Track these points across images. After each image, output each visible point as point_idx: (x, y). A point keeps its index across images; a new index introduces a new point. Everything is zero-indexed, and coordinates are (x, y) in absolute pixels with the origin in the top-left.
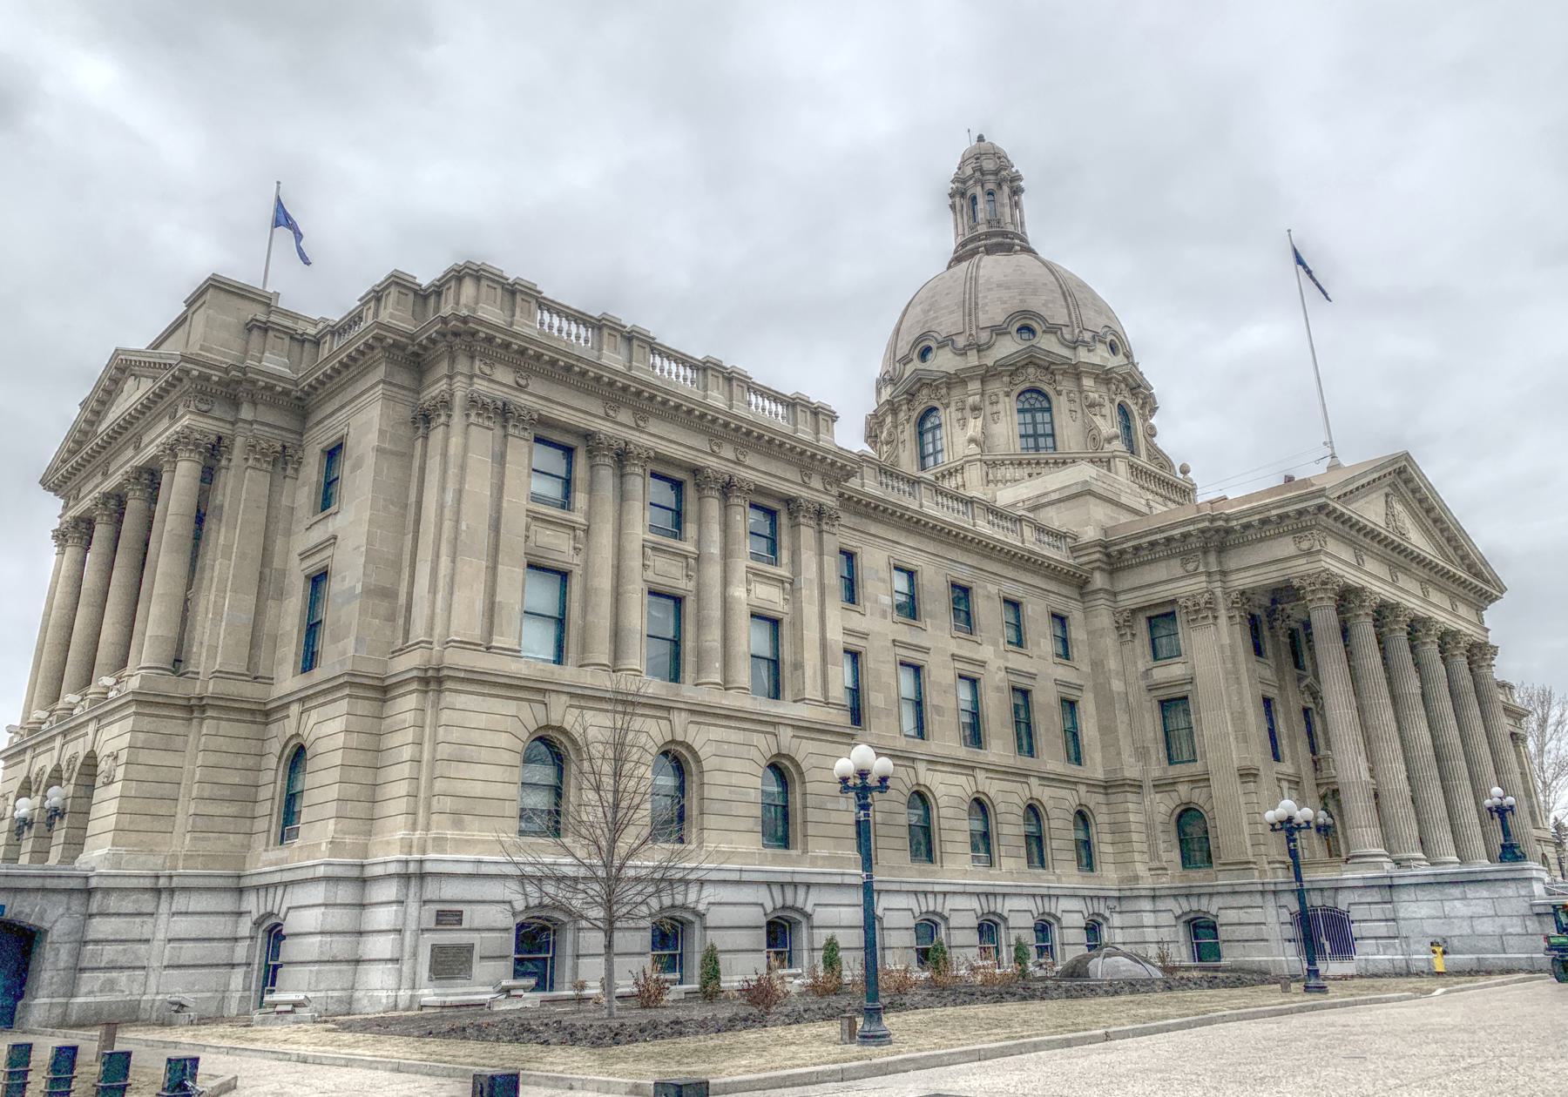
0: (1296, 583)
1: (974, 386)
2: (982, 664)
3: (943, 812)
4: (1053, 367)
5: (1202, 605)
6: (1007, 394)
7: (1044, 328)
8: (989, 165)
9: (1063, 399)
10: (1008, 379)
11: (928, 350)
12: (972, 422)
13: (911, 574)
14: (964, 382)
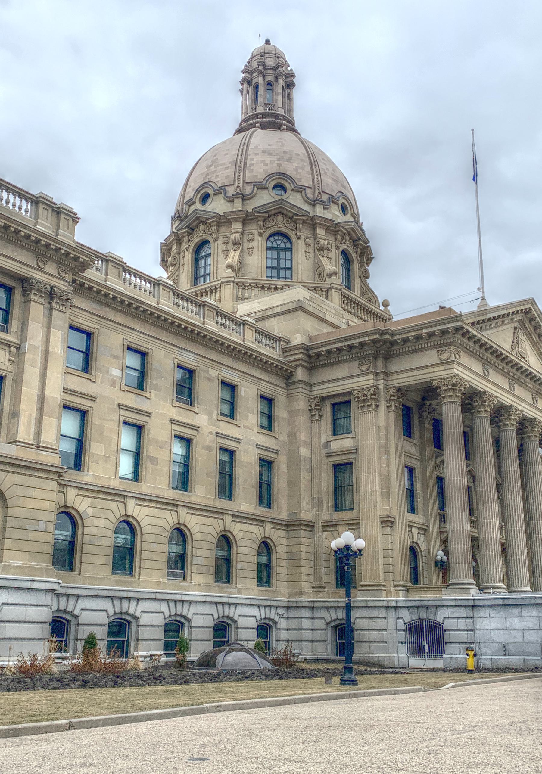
0: (435, 384)
1: (237, 226)
2: (196, 428)
3: (146, 538)
5: (369, 397)
6: (260, 235)
7: (293, 188)
8: (270, 62)
9: (301, 242)
10: (262, 223)
12: (232, 253)
13: (143, 355)
14: (229, 222)
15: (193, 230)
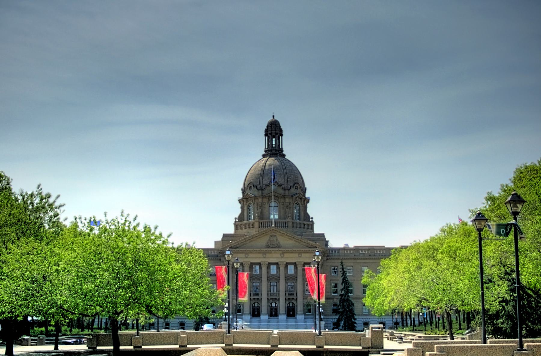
1: (260, 200)
11: (251, 187)
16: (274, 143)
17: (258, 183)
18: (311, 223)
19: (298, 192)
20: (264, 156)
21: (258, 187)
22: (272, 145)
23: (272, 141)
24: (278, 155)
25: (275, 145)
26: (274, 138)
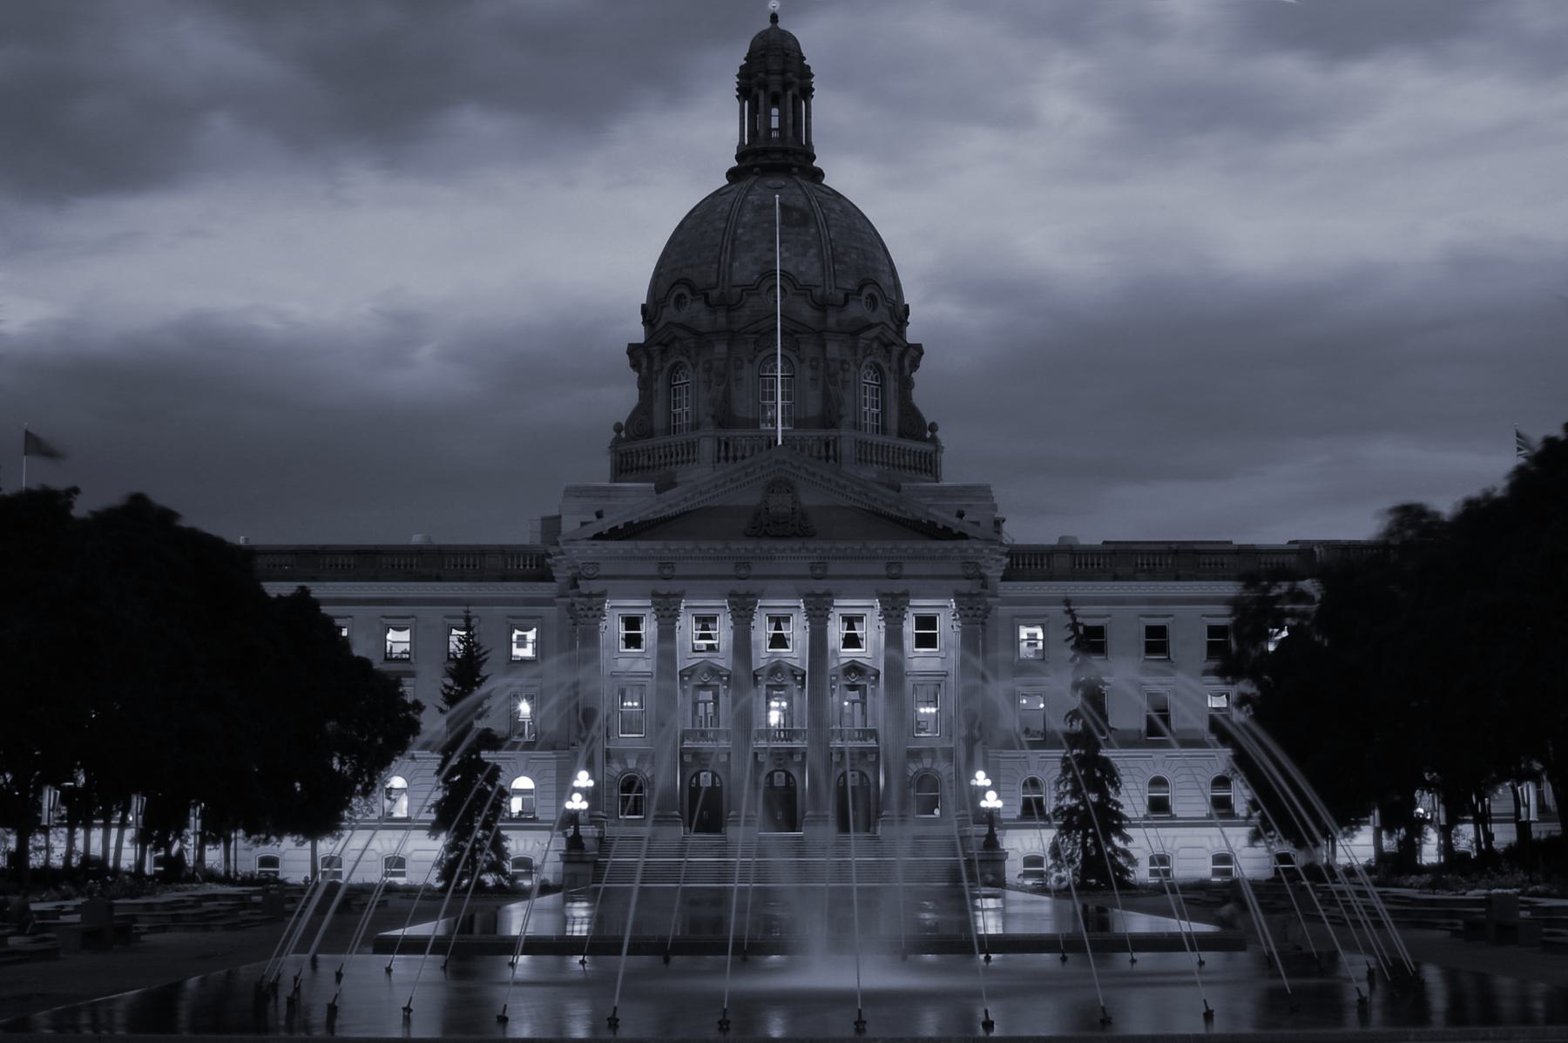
1: (721, 349)
4: (797, 336)
6: (751, 362)
15: (667, 346)
16: (775, 123)
17: (713, 280)
18: (929, 447)
19: (874, 319)
20: (733, 175)
21: (714, 294)
22: (770, 130)
23: (768, 116)
24: (795, 170)
25: (781, 129)
26: (775, 100)
